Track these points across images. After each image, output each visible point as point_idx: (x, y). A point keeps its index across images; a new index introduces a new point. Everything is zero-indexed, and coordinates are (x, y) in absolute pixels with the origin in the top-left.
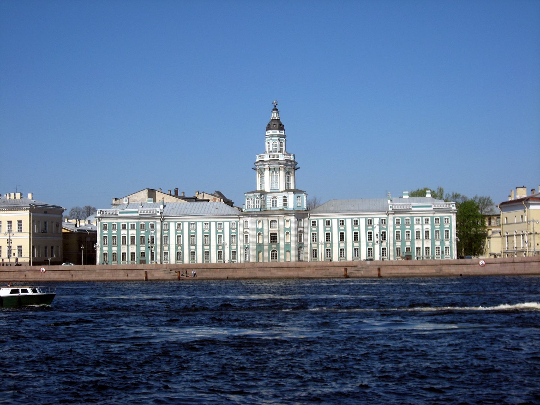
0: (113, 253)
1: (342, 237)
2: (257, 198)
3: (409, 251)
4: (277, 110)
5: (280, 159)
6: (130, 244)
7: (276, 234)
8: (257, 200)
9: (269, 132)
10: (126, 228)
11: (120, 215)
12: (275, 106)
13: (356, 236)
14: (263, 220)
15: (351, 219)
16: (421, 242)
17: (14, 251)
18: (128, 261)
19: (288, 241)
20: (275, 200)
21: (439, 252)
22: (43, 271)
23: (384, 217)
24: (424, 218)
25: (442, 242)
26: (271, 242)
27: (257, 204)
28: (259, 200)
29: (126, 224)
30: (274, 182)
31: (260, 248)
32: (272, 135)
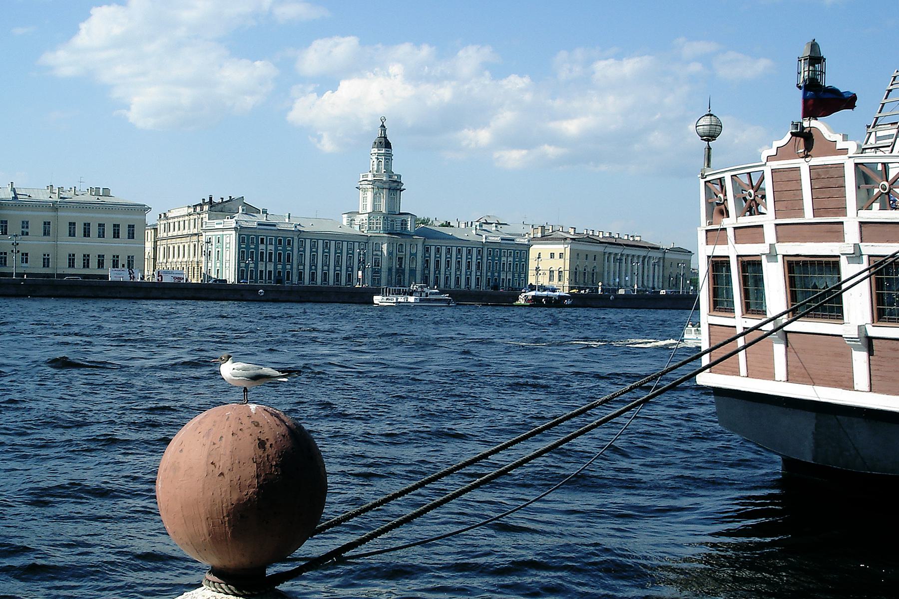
4: (385, 127)
17: (123, 260)
18: (266, 280)
29: (265, 237)
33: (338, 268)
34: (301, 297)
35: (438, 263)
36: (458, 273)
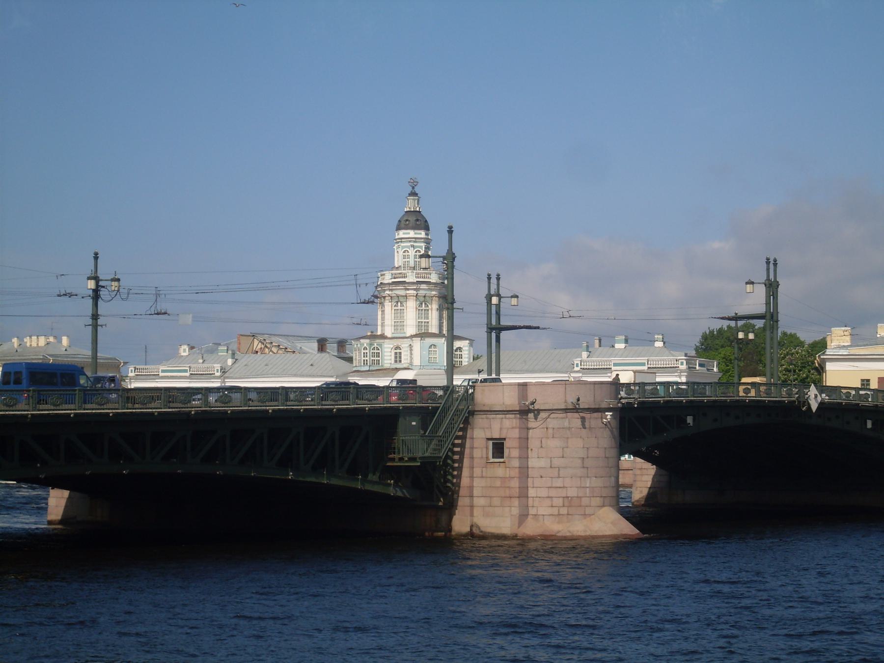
2: (365, 349)
5: (407, 280)
8: (365, 351)
11: (161, 374)
12: (413, 188)
20: (398, 351)
27: (366, 359)
28: (368, 351)
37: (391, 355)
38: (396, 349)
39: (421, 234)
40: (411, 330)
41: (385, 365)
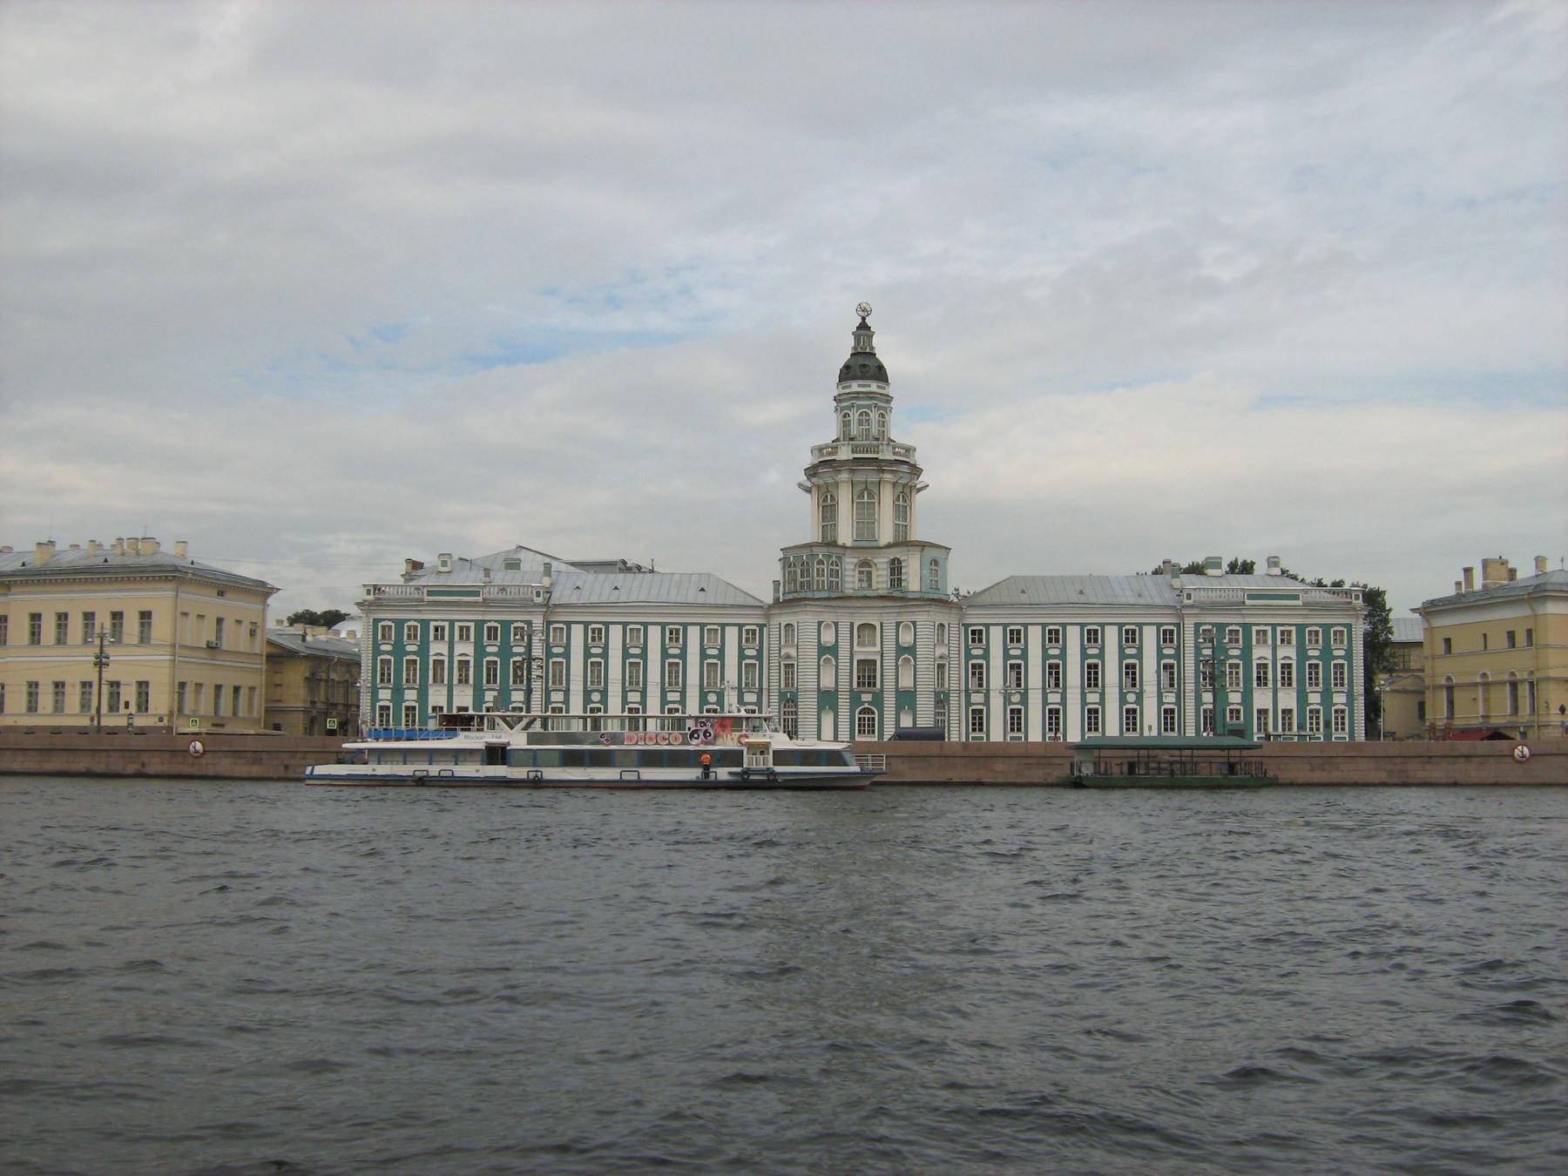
0: (407, 708)
1: (1054, 673)
2: (820, 562)
3: (1238, 718)
5: (880, 456)
6: (455, 681)
7: (875, 661)
8: (821, 567)
9: (850, 386)
10: (446, 638)
11: (427, 598)
12: (863, 319)
13: (1092, 676)
14: (836, 624)
15: (1078, 627)
16: (1271, 695)
17: (129, 694)
19: (906, 682)
21: (1318, 724)
22: (196, 752)
23: (1168, 620)
24: (1279, 629)
25: (1327, 696)
26: (859, 684)
28: (825, 567)
29: (446, 624)
30: (866, 519)
31: (827, 699)
32: (858, 393)
33: (672, 696)
34: (287, 767)
35: (1016, 671)
36: (1093, 698)
37: (854, 576)
38: (860, 567)
39: (884, 388)
40: (886, 535)
41: (847, 591)
